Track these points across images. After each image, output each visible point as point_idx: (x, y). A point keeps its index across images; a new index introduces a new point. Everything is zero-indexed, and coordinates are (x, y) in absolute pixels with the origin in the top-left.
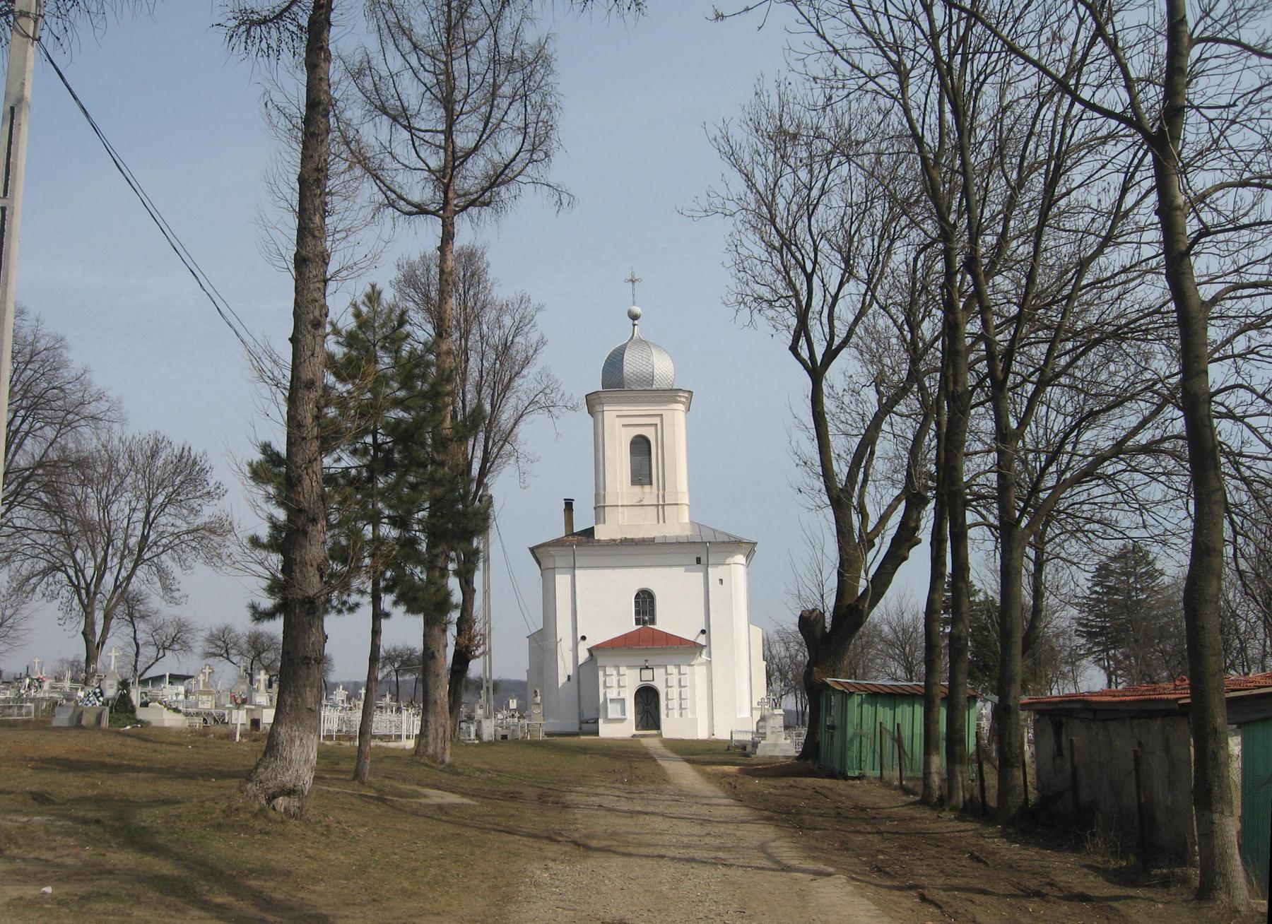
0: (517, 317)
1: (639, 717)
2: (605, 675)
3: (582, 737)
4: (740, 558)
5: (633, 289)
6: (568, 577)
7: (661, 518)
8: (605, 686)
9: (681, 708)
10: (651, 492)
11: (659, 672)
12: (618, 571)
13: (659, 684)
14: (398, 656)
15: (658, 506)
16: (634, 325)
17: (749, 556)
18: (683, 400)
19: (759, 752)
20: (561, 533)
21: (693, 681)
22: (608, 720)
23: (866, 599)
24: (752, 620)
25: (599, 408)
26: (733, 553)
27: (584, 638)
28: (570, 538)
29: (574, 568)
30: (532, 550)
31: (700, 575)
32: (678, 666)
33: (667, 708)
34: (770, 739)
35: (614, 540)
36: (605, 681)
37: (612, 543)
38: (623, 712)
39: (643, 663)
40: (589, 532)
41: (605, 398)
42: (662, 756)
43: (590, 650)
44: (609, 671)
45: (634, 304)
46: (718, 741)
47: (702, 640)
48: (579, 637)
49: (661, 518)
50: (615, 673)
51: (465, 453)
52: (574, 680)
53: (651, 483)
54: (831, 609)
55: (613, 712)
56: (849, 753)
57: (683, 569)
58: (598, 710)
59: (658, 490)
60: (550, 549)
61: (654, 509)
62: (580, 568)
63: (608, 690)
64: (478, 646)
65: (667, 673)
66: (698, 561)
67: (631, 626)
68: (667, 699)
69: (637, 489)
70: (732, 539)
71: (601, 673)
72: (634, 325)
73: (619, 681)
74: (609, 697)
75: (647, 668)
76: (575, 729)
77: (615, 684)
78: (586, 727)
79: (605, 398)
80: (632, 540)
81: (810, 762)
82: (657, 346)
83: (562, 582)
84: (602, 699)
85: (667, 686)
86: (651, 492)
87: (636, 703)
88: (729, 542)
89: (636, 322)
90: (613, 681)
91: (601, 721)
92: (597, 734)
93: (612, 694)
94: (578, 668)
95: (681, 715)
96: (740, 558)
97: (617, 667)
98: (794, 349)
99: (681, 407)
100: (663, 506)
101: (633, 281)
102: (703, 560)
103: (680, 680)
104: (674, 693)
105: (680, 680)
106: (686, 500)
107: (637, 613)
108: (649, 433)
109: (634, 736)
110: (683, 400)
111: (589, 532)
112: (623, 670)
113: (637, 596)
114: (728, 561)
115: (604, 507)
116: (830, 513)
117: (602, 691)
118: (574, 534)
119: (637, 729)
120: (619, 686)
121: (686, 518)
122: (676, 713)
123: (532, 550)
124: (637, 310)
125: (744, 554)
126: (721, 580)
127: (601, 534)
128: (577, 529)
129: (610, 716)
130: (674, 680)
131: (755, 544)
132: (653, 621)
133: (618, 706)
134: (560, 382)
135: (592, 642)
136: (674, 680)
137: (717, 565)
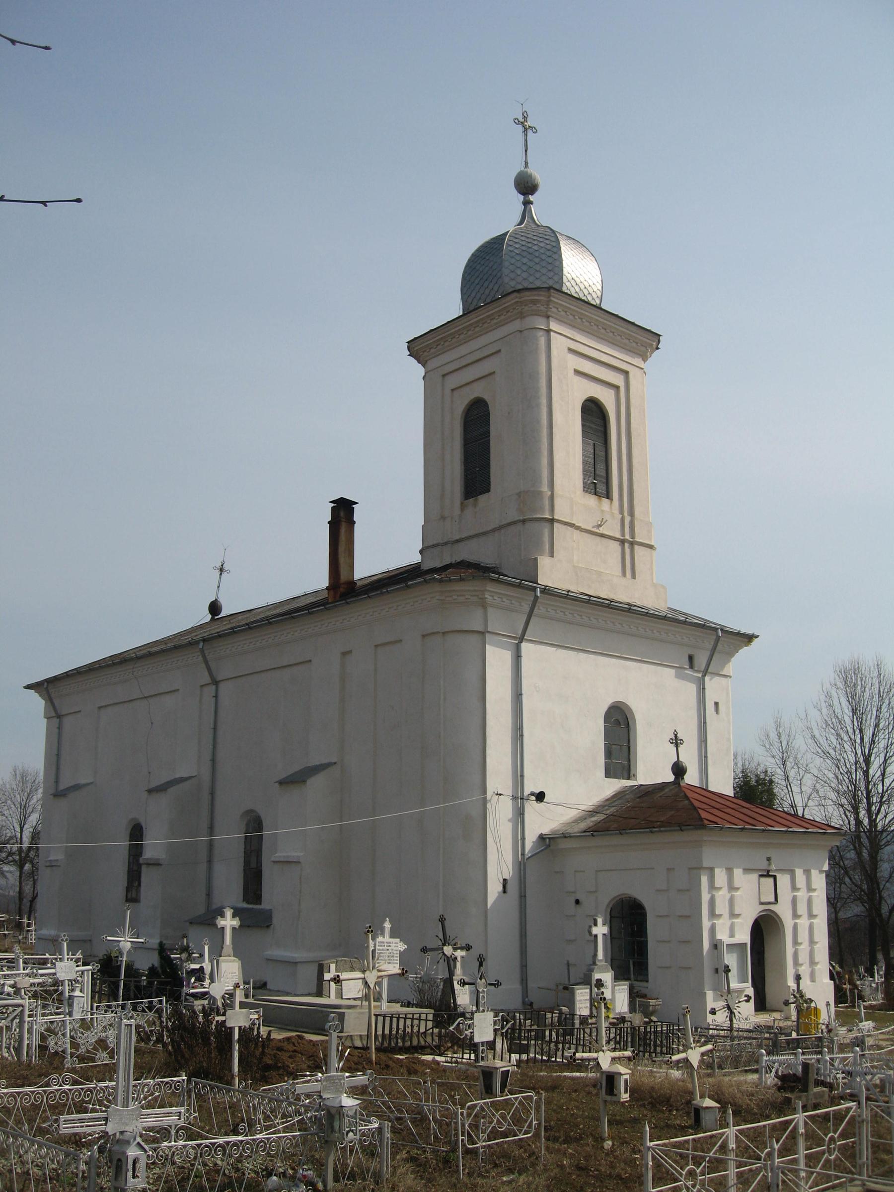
6: (507, 656)
7: (629, 568)
13: (783, 910)
29: (522, 639)
31: (692, 688)
39: (764, 865)
49: (629, 568)
52: (513, 888)
53: (608, 496)
57: (673, 671)
59: (621, 511)
61: (616, 546)
69: (592, 500)
71: (704, 880)
72: (527, 203)
89: (531, 198)
94: (522, 865)
100: (632, 544)
102: (701, 660)
108: (607, 398)
117: (706, 924)
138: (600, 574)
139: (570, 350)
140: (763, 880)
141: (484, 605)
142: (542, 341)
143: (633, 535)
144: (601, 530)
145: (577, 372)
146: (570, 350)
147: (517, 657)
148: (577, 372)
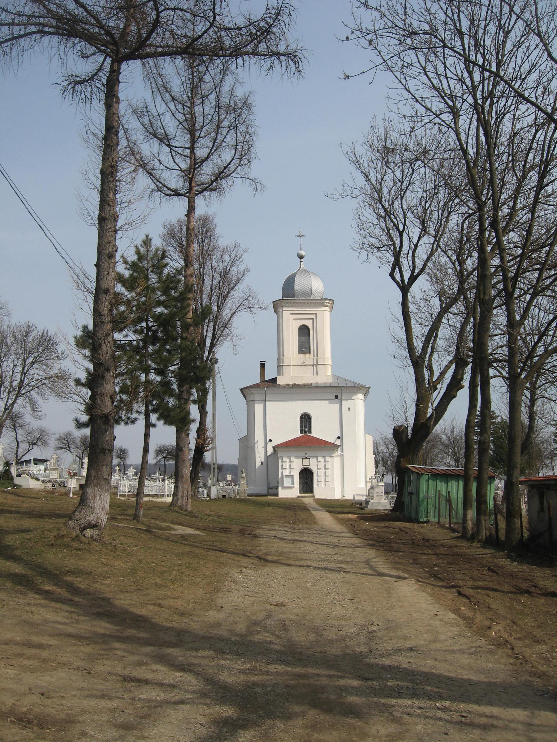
0: (233, 256)
1: (302, 486)
2: (282, 462)
3: (269, 497)
4: (361, 396)
5: (301, 241)
6: (262, 406)
7: (316, 373)
8: (282, 468)
9: (325, 481)
10: (310, 358)
11: (313, 461)
12: (290, 402)
13: (313, 467)
14: (165, 450)
15: (313, 365)
16: (301, 262)
17: (365, 395)
18: (329, 305)
19: (370, 507)
20: (258, 380)
21: (333, 465)
22: (284, 488)
23: (432, 419)
24: (367, 431)
25: (280, 309)
26: (356, 393)
27: (270, 441)
28: (263, 383)
29: (265, 401)
30: (241, 390)
31: (338, 405)
32: (324, 457)
33: (318, 481)
34: (376, 500)
35: (288, 385)
36: (282, 466)
37: (287, 387)
38: (293, 482)
39: (304, 455)
40: (274, 380)
41: (284, 303)
42: (313, 509)
43: (274, 447)
44: (285, 459)
45: (301, 249)
46: (346, 500)
47: (338, 442)
48: (268, 440)
49: (316, 373)
50: (288, 460)
51: (202, 334)
52: (264, 464)
53: (310, 353)
54: (412, 425)
55: (287, 482)
56: (421, 508)
57: (328, 402)
58: (278, 482)
59: (314, 356)
60: (251, 389)
61: (311, 367)
62: (269, 400)
63: (284, 470)
64: (209, 444)
65: (318, 461)
66: (337, 397)
67: (298, 434)
68: (318, 476)
69: (302, 356)
70: (356, 385)
71: (280, 461)
73: (290, 465)
74: (285, 474)
75: (306, 458)
76: (265, 492)
77: (288, 467)
78: (271, 491)
79: (284, 303)
80: (299, 385)
81: (398, 513)
82: (314, 274)
83: (258, 408)
84: (280, 476)
85: (318, 469)
86: (310, 358)
87: (300, 478)
88: (354, 386)
89: (302, 260)
90: (287, 465)
91: (280, 488)
92: (277, 495)
93: (286, 473)
94: (267, 458)
95: (326, 485)
96: (361, 396)
97: (289, 457)
98: (392, 275)
99: (327, 309)
101: (300, 236)
102: (339, 397)
103: (325, 465)
104: (322, 472)
105: (325, 465)
106: (329, 362)
107: (301, 427)
108: (309, 324)
109: (298, 497)
110: (329, 305)
111: (274, 380)
112: (293, 459)
113: (301, 417)
114: (353, 398)
115: (283, 366)
116: (411, 370)
118: (265, 381)
119: (300, 493)
120: (290, 468)
121: (329, 373)
122: (322, 484)
123: (241, 390)
124: (302, 253)
125: (363, 394)
126: (349, 408)
127: (281, 381)
128: (267, 378)
129: (285, 485)
130: (321, 465)
131: (369, 388)
132: (310, 431)
133: (289, 480)
134: (256, 293)
135: (274, 443)
136: (321, 465)
137: (347, 399)
138: (302, 377)
139: (291, 314)
140: (304, 460)
141: (254, 394)
142: (281, 314)
143: (317, 362)
144: (305, 364)
145: (295, 319)
146: (291, 314)
147: (265, 406)
148: (295, 319)
